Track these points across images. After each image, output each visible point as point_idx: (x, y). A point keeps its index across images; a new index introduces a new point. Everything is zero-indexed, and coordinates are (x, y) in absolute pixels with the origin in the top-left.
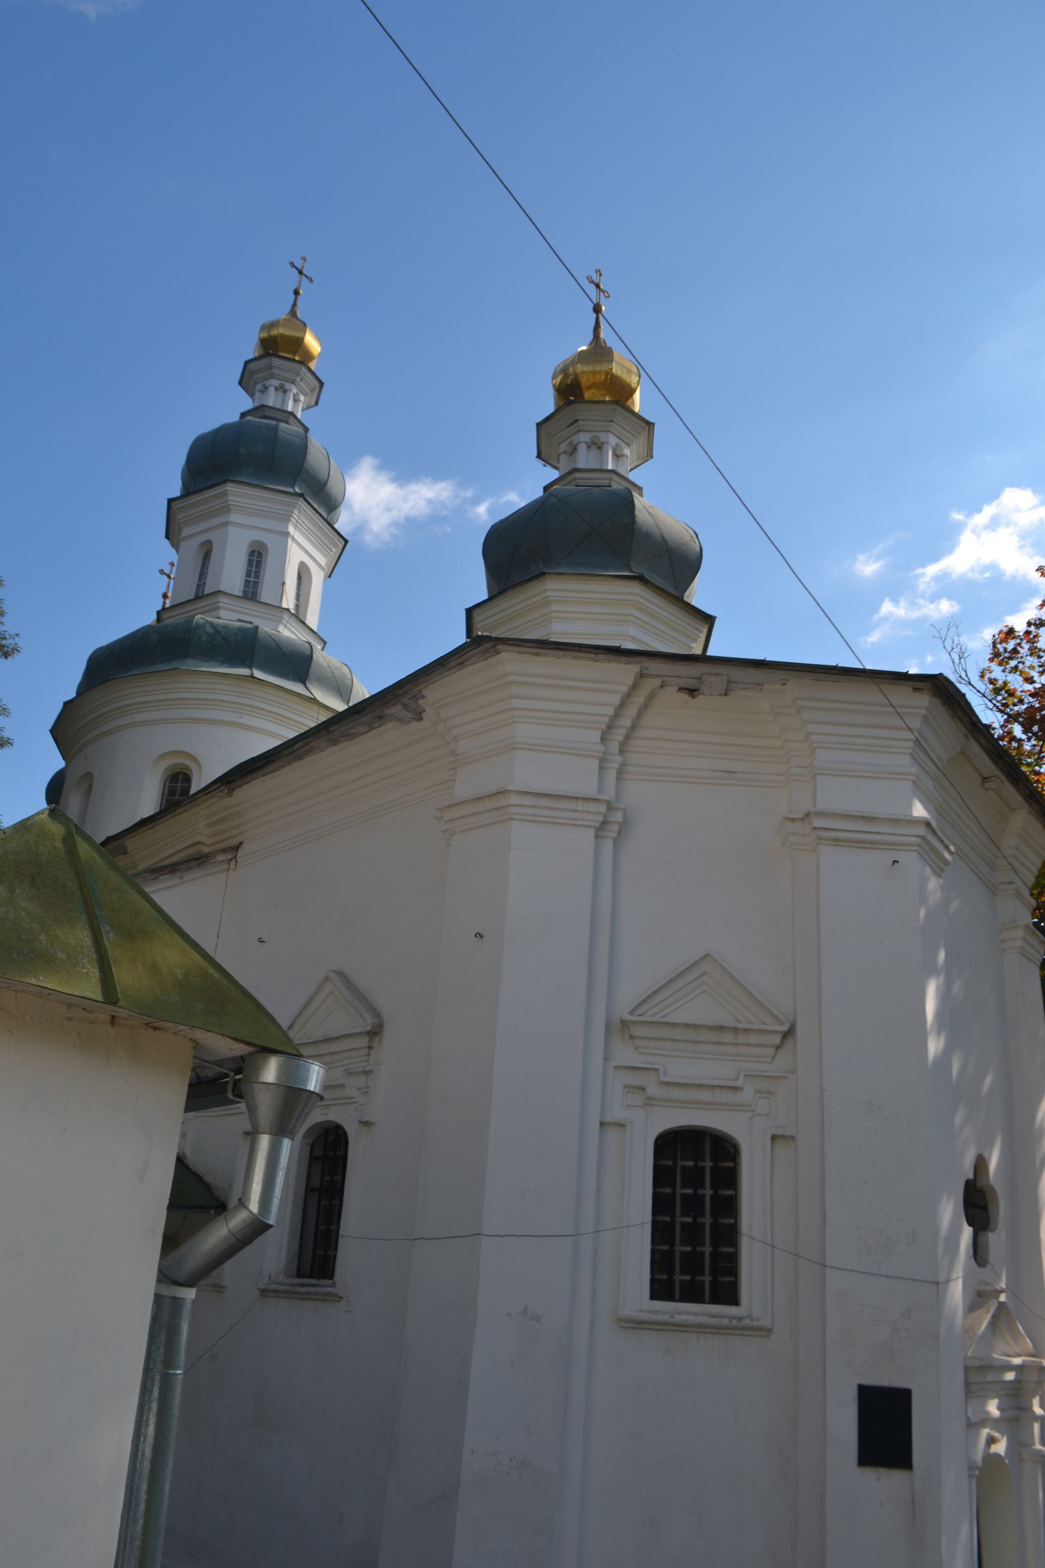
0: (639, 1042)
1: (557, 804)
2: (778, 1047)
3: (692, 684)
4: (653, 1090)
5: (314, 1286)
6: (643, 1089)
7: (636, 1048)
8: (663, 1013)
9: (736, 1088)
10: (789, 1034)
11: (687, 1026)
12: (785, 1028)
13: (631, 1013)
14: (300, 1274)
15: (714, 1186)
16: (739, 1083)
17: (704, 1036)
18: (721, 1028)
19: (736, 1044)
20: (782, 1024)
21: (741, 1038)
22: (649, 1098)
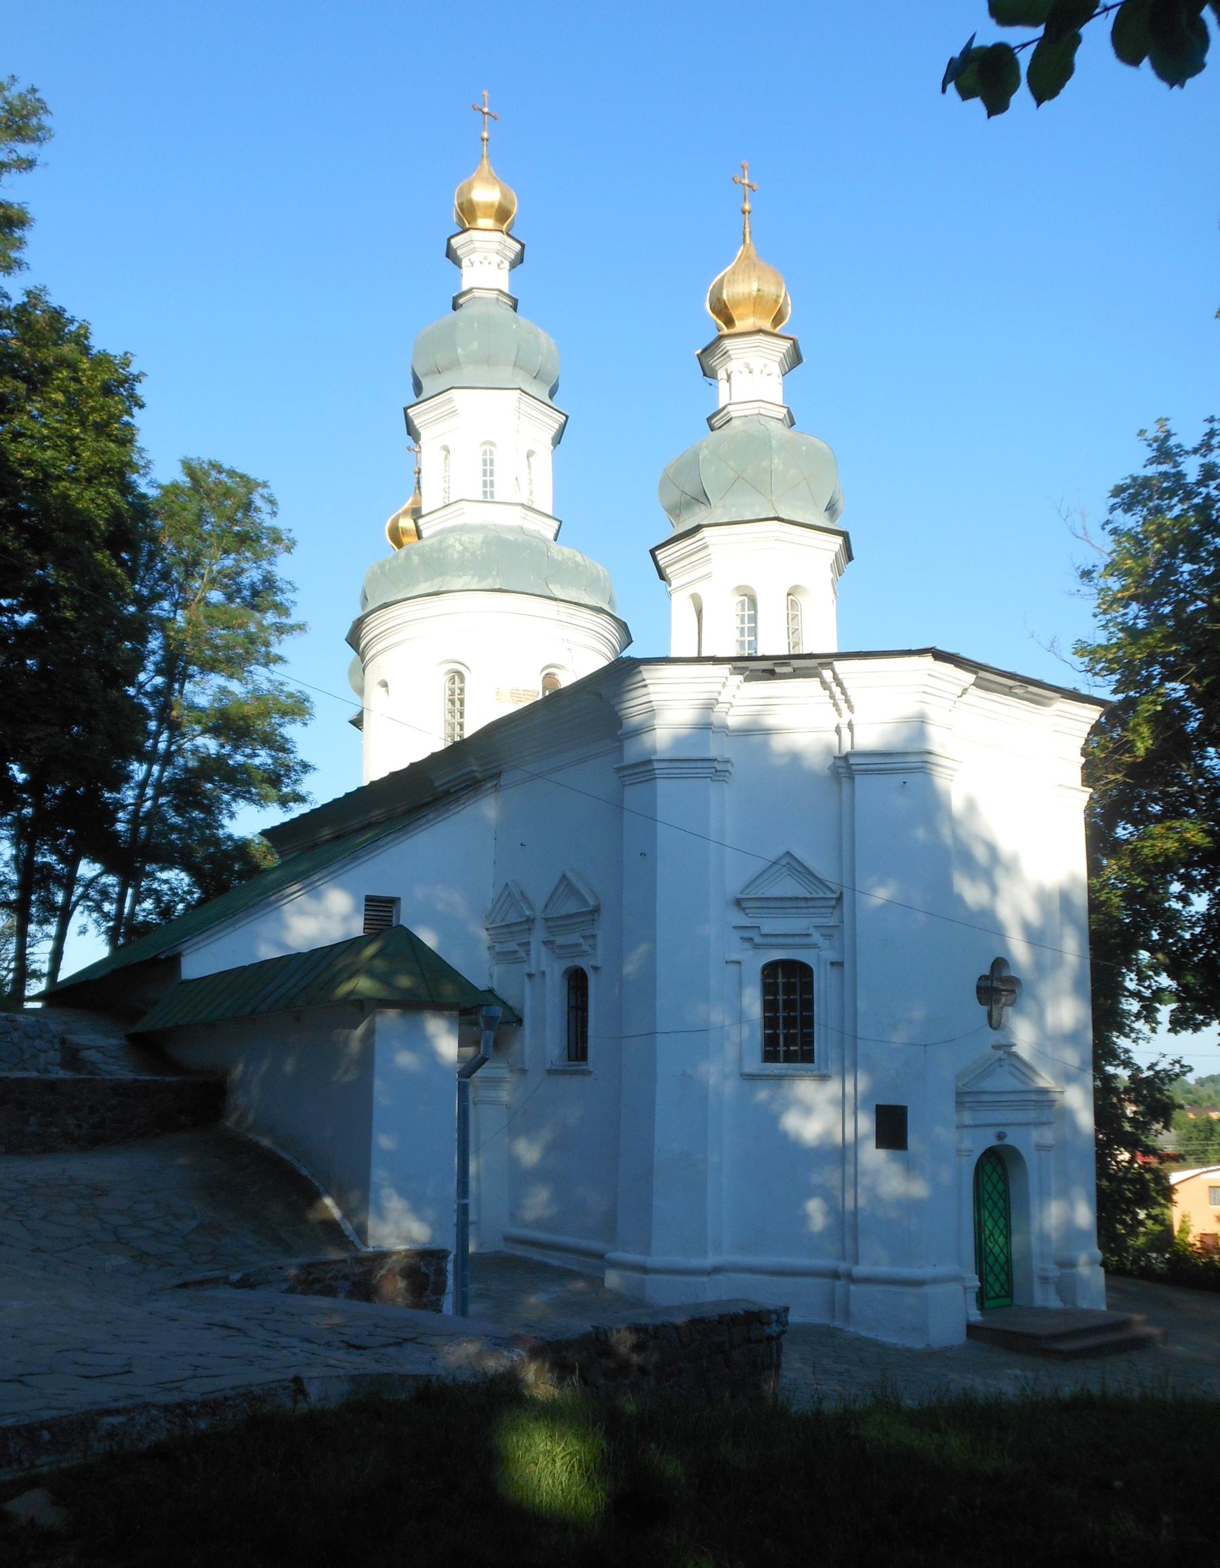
0: (747, 911)
1: (684, 765)
2: (834, 907)
3: (771, 667)
4: (758, 940)
5: (577, 1066)
6: (752, 939)
7: (747, 914)
8: (761, 892)
9: (808, 935)
10: (839, 899)
11: (776, 899)
12: (835, 896)
13: (742, 892)
14: (570, 1060)
15: (776, 1001)
16: (808, 932)
17: (787, 904)
18: (797, 899)
19: (808, 907)
20: (834, 892)
21: (811, 904)
22: (755, 944)
